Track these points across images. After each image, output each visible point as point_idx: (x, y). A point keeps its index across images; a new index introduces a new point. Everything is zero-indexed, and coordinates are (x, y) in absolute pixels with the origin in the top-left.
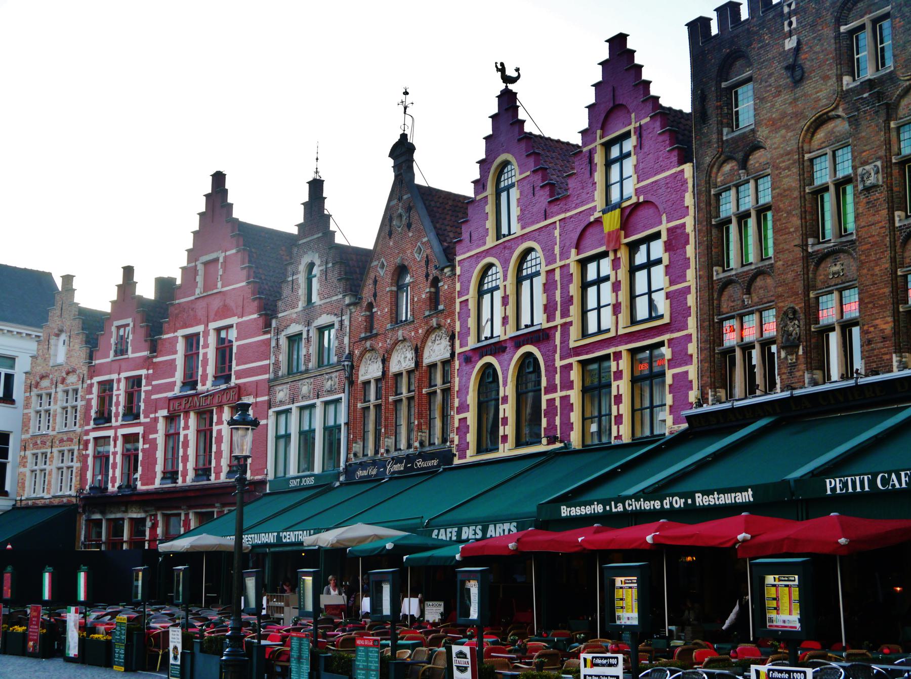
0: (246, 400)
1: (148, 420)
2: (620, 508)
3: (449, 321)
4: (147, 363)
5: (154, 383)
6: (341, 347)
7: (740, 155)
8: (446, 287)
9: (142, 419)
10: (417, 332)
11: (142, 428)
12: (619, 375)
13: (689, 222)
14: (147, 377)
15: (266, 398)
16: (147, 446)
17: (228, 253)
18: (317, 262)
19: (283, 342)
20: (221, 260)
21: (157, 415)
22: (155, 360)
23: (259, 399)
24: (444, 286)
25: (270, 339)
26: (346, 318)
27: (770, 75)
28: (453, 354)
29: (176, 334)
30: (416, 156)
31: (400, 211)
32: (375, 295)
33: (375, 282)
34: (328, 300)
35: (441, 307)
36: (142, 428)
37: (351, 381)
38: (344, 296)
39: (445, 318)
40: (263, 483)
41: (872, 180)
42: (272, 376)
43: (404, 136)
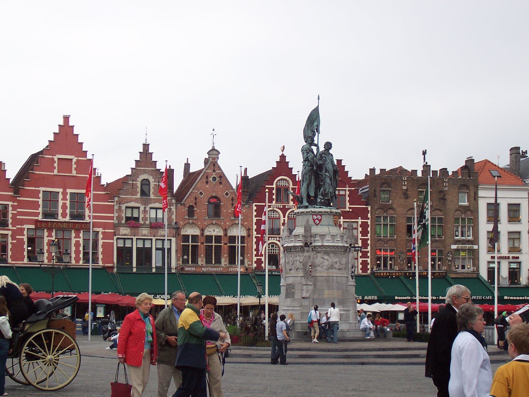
0: (97, 229)
1: (15, 228)
4: (12, 199)
5: (18, 210)
7: (385, 209)
9: (10, 227)
11: (11, 232)
13: (369, 221)
14: (12, 206)
15: (112, 231)
16: (15, 241)
17: (80, 158)
18: (151, 179)
19: (123, 207)
20: (75, 159)
21: (23, 227)
22: (18, 198)
23: (106, 231)
25: (114, 205)
26: (173, 209)
28: (249, 236)
29: (37, 189)
30: (219, 156)
32: (196, 204)
33: (196, 199)
36: (11, 232)
37: (179, 234)
40: (113, 268)
42: (115, 221)
43: (214, 146)
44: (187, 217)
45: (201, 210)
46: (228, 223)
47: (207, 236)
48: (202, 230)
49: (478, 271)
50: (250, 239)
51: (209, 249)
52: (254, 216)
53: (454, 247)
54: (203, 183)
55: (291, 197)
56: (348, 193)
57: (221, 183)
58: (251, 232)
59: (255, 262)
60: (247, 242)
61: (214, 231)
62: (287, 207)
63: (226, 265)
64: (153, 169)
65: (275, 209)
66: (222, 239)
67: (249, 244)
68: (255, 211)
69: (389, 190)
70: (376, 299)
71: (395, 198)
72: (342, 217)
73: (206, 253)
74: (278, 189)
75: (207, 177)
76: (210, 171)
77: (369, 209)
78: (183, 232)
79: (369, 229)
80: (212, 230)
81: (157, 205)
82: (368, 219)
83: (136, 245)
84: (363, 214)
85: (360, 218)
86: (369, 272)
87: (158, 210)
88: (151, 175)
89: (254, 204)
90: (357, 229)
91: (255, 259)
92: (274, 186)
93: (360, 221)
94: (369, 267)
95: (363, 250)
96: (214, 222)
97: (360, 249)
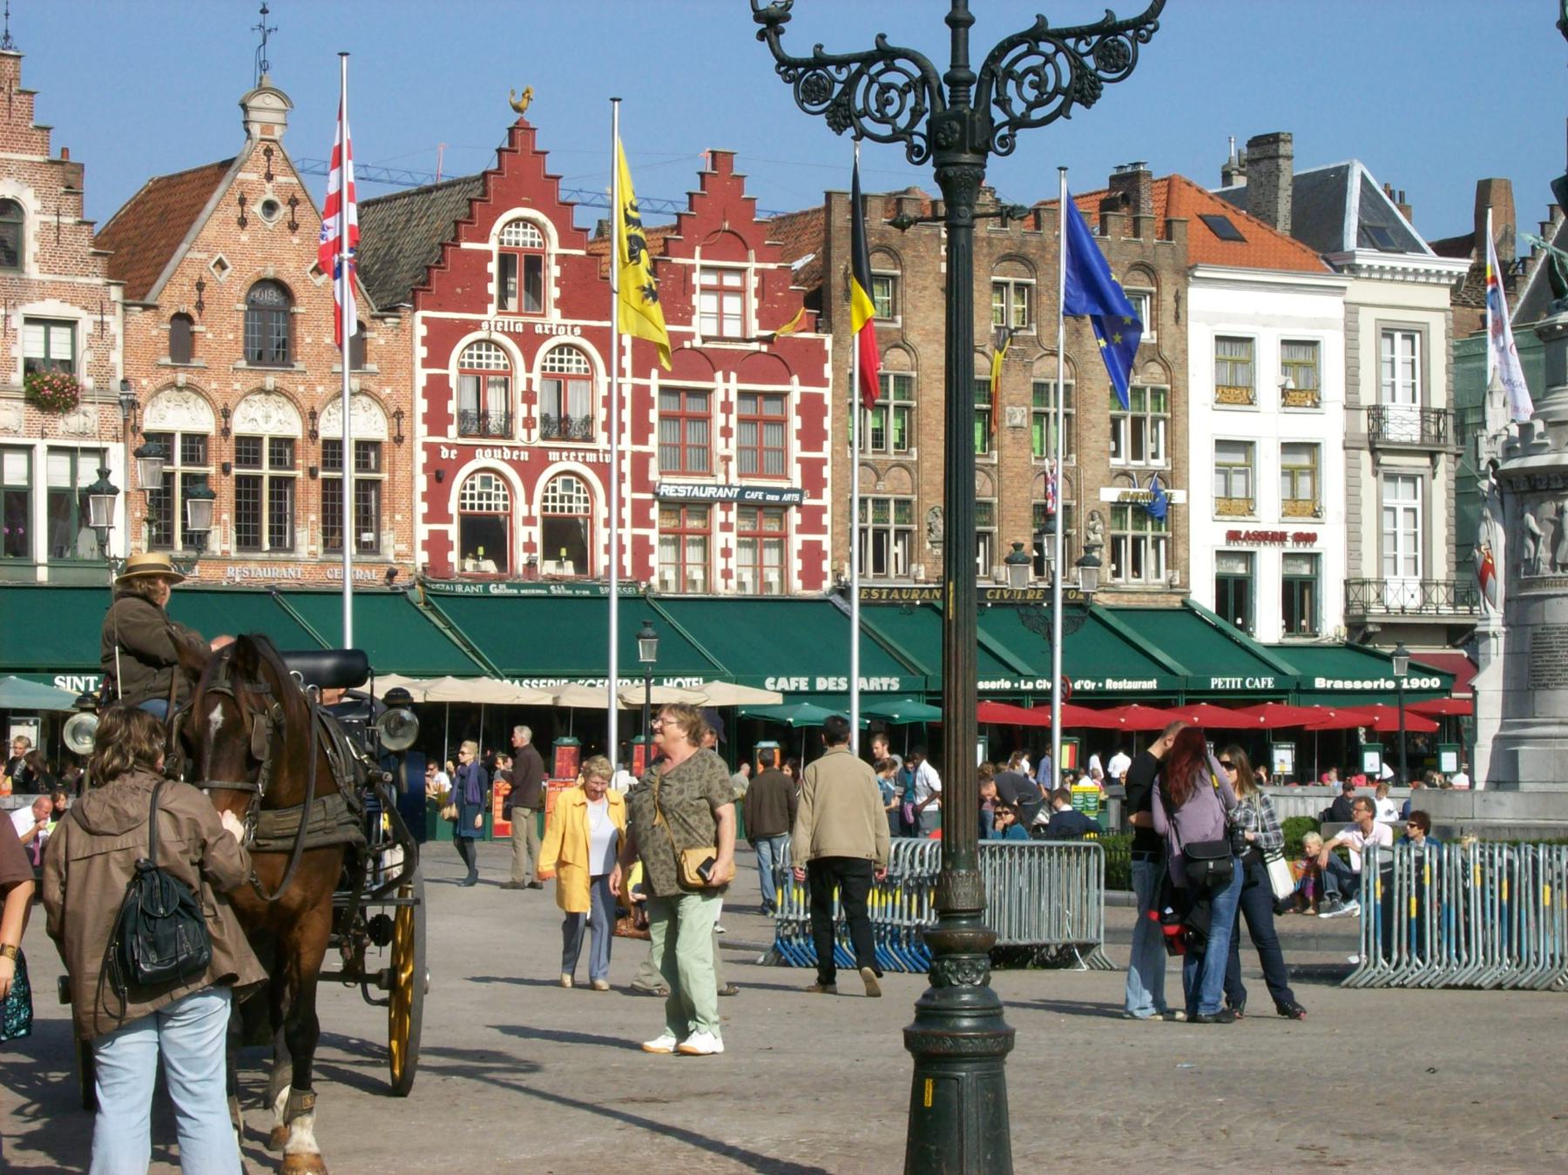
2: (1030, 686)
3: (388, 390)
6: (102, 368)
8: (382, 342)
10: (311, 386)
12: (726, 527)
18: (30, 201)
24: (378, 338)
26: (115, 323)
27: (925, 288)
28: (399, 440)
31: (270, 196)
32: (200, 306)
33: (200, 286)
34: (63, 278)
35: (371, 367)
37: (136, 429)
38: (109, 284)
39: (380, 384)
41: (1017, 421)
44: (168, 361)
45: (221, 333)
46: (320, 389)
47: (240, 439)
48: (226, 414)
49: (1187, 585)
50: (401, 452)
51: (247, 488)
52: (418, 363)
53: (1110, 494)
54: (225, 222)
55: (554, 292)
56: (753, 282)
57: (293, 227)
58: (403, 422)
59: (426, 545)
60: (393, 463)
61: (268, 417)
62: (538, 330)
63: (314, 554)
64: (38, 158)
65: (497, 337)
66: (300, 452)
67: (401, 475)
68: (425, 341)
69: (894, 277)
70: (896, 687)
71: (915, 307)
72: (733, 376)
73: (238, 506)
74: (506, 261)
75: (242, 202)
76: (253, 177)
77: (828, 341)
78: (152, 421)
79: (827, 423)
80: (259, 415)
81: (51, 308)
82: (824, 383)
83: (50, 473)
84: (808, 363)
85: (795, 379)
86: (827, 584)
87: (54, 330)
88: (33, 183)
89: (420, 314)
90: (782, 422)
91: (422, 531)
92: (493, 246)
93: (796, 390)
94: (827, 566)
95: (806, 502)
96: (270, 381)
97: (796, 497)
